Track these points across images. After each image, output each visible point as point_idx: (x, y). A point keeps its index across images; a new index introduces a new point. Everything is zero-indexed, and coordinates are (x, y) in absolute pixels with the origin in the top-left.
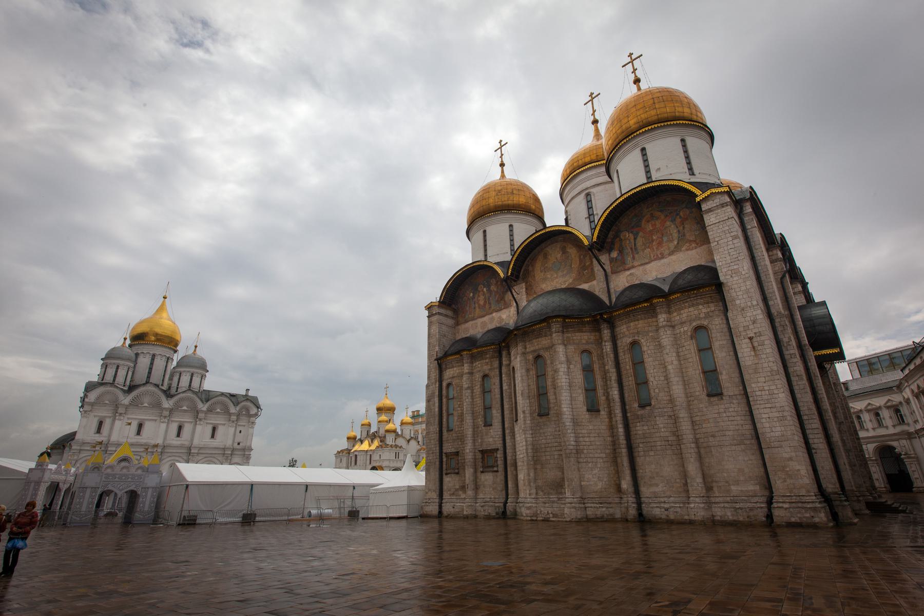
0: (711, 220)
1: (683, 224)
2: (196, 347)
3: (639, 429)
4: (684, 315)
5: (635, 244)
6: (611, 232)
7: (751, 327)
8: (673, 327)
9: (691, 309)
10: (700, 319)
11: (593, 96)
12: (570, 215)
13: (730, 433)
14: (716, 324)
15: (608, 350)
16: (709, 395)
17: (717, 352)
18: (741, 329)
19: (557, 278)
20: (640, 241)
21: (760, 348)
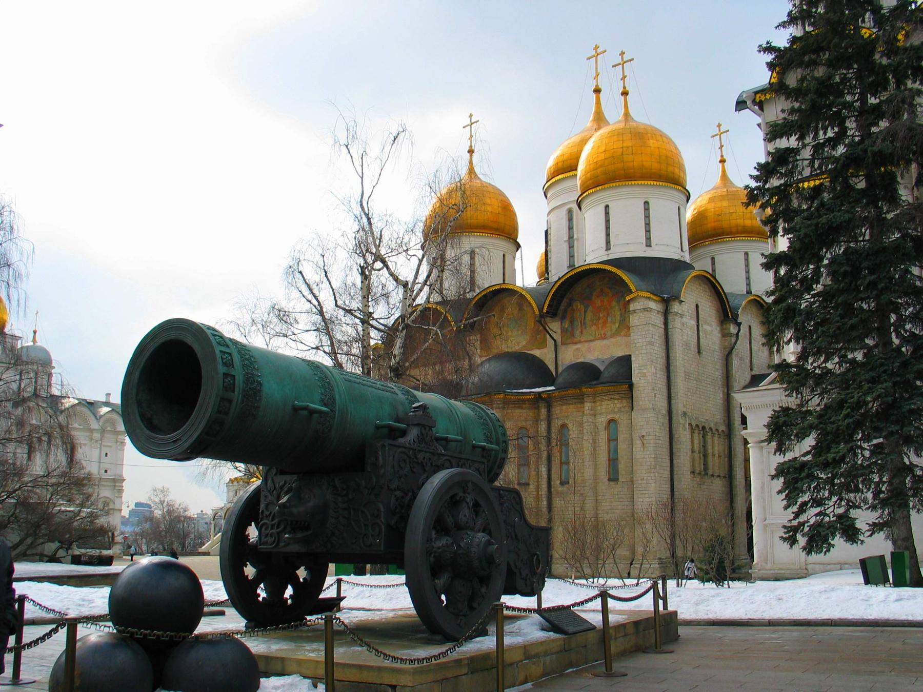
0: (635, 321)
1: (625, 307)
2: (35, 332)
3: (558, 503)
4: (604, 407)
5: (584, 318)
6: (565, 300)
7: (645, 427)
8: (595, 415)
9: (609, 402)
10: (614, 412)
11: (599, 50)
12: (550, 228)
13: (618, 511)
14: (622, 419)
15: (543, 429)
16: (609, 480)
17: (621, 444)
18: (638, 427)
19: (512, 336)
20: (589, 316)
21: (647, 445)
